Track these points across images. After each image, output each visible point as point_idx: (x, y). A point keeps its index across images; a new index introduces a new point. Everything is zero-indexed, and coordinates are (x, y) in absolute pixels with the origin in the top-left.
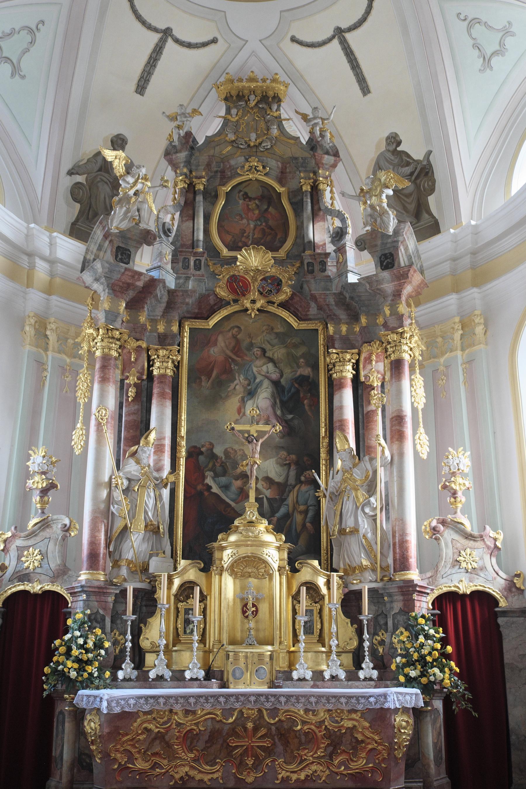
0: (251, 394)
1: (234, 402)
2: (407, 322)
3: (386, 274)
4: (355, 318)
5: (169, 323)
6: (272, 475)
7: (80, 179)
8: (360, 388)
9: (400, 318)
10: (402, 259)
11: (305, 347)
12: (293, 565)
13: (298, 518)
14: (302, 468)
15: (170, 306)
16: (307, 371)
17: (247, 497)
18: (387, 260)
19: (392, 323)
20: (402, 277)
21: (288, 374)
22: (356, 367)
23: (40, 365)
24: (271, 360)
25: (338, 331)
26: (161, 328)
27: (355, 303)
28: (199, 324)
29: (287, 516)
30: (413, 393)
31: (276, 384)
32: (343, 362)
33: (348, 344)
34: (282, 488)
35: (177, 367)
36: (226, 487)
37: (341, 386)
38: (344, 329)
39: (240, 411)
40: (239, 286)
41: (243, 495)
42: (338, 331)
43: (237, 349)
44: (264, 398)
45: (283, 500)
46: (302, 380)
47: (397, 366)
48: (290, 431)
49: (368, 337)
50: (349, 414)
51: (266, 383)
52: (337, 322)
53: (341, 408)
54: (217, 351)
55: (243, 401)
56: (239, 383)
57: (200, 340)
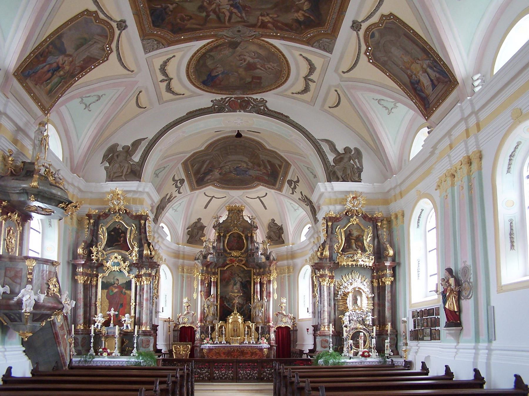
0: (235, 284)
1: (231, 286)
2: (272, 271)
3: (267, 262)
4: (260, 268)
5: (215, 269)
6: (240, 302)
7: (190, 229)
8: (261, 284)
9: (271, 271)
10: (271, 258)
11: (248, 274)
12: (245, 321)
13: (246, 311)
14: (247, 301)
15: (215, 266)
16: (249, 279)
17: (234, 307)
18: (268, 258)
19: (269, 272)
20: (271, 263)
21: (244, 280)
22: (260, 279)
23: (183, 277)
24: (240, 277)
25: (256, 271)
26: (213, 271)
27: (260, 266)
28: (222, 269)
29: (243, 311)
30: (274, 286)
31: (241, 282)
32: (257, 278)
33: (259, 274)
34: (242, 305)
35: (217, 279)
36: (229, 305)
37: (257, 284)
38: (258, 271)
39: (233, 288)
40: (232, 261)
41: (233, 306)
42: (256, 271)
43: (232, 274)
44: (238, 285)
45: (242, 308)
46: (247, 281)
47: (269, 281)
48: (244, 293)
49: (264, 274)
50: (259, 290)
51: (239, 282)
52: (256, 269)
53: (257, 288)
54: (227, 275)
55: (233, 287)
56: (232, 282)
57: (222, 272)
